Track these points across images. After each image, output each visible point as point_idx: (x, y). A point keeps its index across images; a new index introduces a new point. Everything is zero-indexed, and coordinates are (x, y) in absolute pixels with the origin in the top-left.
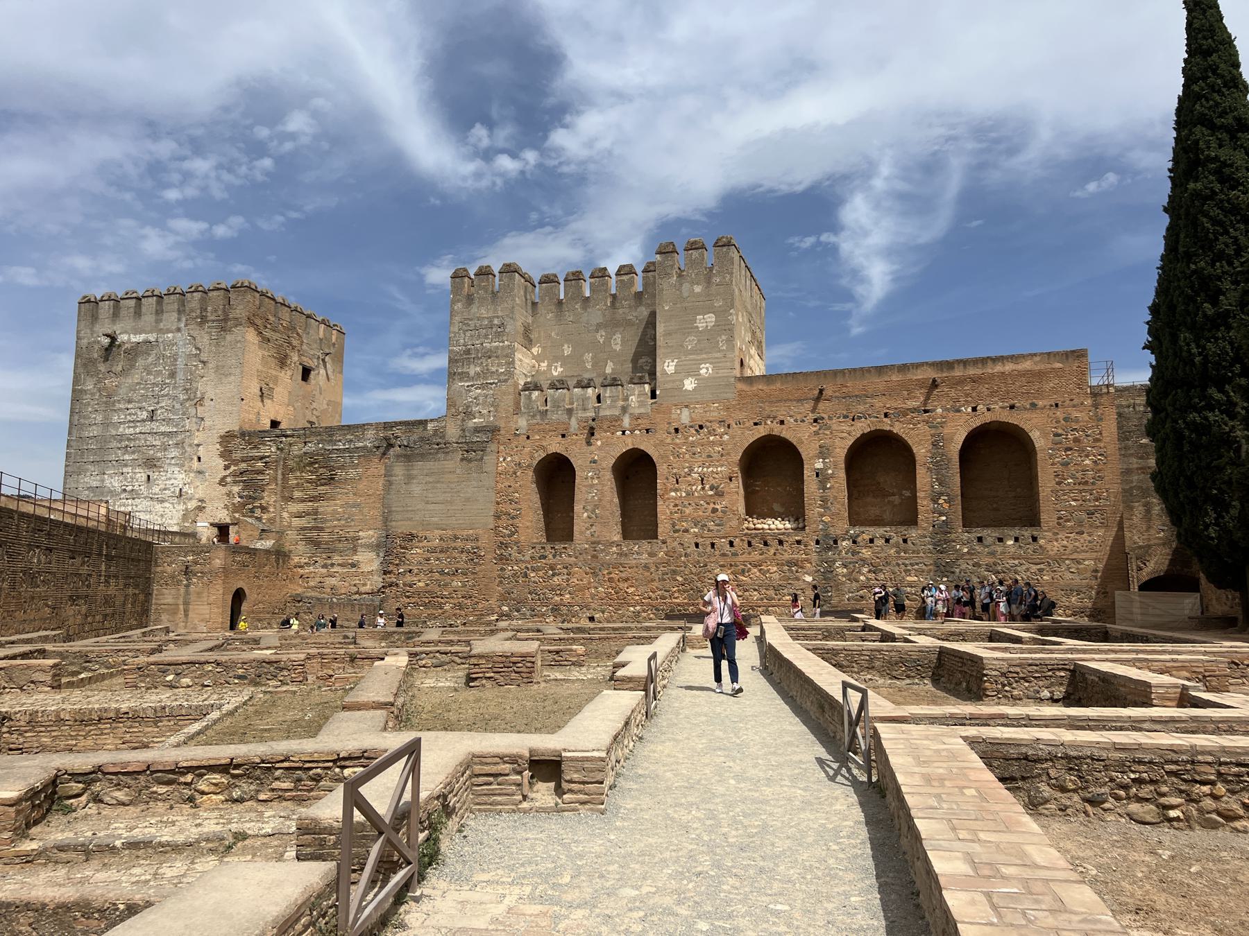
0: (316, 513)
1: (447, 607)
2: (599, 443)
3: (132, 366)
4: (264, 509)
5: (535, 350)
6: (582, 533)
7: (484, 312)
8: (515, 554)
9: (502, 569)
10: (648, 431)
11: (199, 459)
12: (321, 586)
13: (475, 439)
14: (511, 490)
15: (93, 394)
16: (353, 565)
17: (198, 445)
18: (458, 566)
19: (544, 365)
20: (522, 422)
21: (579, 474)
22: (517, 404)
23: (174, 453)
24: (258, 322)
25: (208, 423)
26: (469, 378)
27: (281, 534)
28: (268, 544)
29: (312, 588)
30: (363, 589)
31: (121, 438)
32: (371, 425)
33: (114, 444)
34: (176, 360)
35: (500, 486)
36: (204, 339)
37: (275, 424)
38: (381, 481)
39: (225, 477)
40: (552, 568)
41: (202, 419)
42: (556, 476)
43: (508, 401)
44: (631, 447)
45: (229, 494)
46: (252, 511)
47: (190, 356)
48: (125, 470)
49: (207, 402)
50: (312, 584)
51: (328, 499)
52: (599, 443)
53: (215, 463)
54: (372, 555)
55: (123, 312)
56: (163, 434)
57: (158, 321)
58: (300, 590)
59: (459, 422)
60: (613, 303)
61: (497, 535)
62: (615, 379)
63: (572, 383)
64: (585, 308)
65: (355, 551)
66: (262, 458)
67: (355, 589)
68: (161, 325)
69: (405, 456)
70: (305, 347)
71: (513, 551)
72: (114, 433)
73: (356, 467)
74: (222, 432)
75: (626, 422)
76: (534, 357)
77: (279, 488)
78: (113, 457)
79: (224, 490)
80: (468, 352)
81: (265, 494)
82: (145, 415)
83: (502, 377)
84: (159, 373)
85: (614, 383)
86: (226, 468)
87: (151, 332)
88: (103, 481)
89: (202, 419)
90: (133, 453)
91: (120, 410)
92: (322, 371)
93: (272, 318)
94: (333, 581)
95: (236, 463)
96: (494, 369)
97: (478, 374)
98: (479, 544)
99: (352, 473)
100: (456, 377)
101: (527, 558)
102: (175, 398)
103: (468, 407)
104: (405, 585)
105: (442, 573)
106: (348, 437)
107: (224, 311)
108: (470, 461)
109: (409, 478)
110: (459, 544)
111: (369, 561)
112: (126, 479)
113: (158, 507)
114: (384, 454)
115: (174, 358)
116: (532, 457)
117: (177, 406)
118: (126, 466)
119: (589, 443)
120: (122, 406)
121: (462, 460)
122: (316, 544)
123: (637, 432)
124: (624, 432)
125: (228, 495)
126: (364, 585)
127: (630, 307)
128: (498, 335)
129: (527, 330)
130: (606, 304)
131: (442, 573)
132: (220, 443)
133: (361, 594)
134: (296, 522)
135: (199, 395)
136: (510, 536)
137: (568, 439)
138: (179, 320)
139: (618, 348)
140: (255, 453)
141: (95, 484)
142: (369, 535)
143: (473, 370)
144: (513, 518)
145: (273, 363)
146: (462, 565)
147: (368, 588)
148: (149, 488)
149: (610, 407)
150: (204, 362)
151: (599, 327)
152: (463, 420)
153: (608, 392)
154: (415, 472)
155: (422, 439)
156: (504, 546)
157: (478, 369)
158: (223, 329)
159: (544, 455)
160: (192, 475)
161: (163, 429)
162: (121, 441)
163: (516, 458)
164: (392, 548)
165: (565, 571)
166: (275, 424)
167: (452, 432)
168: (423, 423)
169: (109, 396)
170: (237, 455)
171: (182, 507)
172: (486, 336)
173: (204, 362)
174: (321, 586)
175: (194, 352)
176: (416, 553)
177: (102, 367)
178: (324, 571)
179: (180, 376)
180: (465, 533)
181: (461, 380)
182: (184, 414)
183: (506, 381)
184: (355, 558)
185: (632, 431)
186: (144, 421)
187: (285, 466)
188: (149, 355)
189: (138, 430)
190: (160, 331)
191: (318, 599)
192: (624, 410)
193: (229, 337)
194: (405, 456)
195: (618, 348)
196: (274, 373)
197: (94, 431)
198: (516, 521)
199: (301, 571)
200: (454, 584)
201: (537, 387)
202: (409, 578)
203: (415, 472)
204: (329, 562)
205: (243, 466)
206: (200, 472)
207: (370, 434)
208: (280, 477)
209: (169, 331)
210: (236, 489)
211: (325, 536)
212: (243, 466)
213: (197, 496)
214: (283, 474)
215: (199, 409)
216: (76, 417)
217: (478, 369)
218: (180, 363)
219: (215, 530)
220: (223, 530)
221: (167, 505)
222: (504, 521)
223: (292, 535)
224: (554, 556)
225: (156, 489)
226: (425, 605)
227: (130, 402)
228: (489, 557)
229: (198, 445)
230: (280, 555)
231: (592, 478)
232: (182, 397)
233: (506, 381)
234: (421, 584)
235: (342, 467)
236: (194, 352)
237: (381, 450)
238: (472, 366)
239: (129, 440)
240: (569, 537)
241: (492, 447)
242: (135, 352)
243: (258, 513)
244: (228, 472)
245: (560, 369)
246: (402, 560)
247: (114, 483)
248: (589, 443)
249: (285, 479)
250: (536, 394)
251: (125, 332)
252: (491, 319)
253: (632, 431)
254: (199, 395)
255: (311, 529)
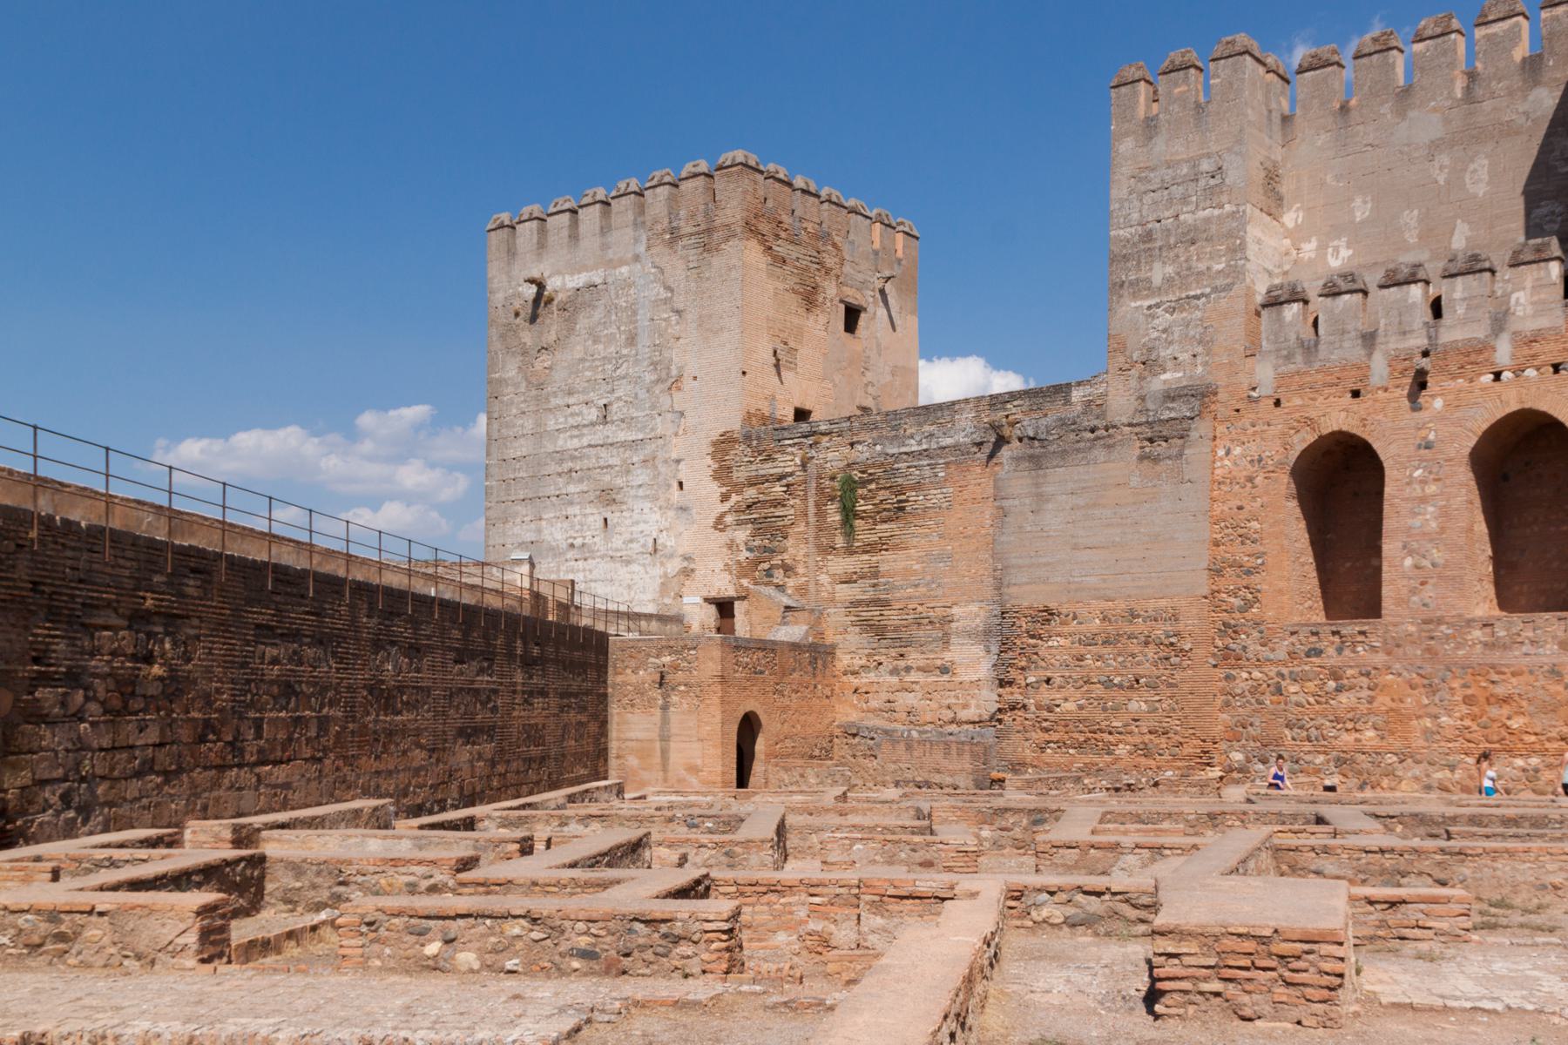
0: (876, 575)
1: (1122, 750)
2: (1438, 403)
3: (571, 330)
4: (788, 569)
5: (1290, 218)
6: (1400, 602)
7: (1179, 149)
8: (1254, 648)
9: (1228, 678)
10: (1556, 368)
11: (681, 484)
12: (889, 708)
13: (1166, 415)
14: (1244, 514)
15: (517, 385)
16: (944, 670)
17: (678, 461)
18: (1140, 670)
19: (1309, 248)
20: (1265, 374)
21: (1387, 472)
22: (1253, 336)
23: (641, 476)
24: (764, 227)
25: (690, 420)
26: (1152, 291)
27: (817, 616)
28: (793, 632)
29: (873, 711)
30: (964, 715)
31: (561, 457)
32: (966, 401)
33: (553, 468)
34: (635, 313)
35: (1218, 508)
36: (676, 266)
37: (801, 415)
38: (988, 512)
39: (722, 515)
40: (1335, 676)
41: (682, 414)
42: (1340, 486)
43: (1233, 332)
44: (1514, 407)
45: (731, 545)
46: (769, 573)
47: (657, 303)
48: (571, 511)
49: (688, 383)
50: (874, 704)
51: (896, 547)
52: (1438, 403)
53: (706, 492)
54: (978, 650)
55: (552, 239)
56: (623, 444)
57: (605, 247)
58: (854, 716)
59: (1133, 383)
60: (1468, 90)
61: (1216, 608)
62: (1475, 258)
63: (1372, 279)
64: (1401, 113)
65: (946, 641)
66: (781, 477)
67: (949, 715)
68: (610, 254)
69: (1031, 458)
70: (847, 269)
71: (1250, 642)
72: (550, 448)
73: (939, 485)
74: (715, 436)
75: (1503, 353)
76: (1288, 234)
77: (812, 532)
78: (552, 491)
79: (723, 538)
80: (1148, 237)
81: (789, 543)
82: (593, 414)
83: (1220, 282)
84: (611, 339)
85: (1474, 266)
86: (725, 498)
87: (595, 267)
88: (539, 531)
89: (682, 414)
90: (581, 480)
91: (558, 408)
92: (882, 312)
93: (786, 218)
94: (909, 700)
95: (738, 488)
96: (1202, 266)
97: (1169, 281)
98: (1181, 627)
99: (936, 497)
100: (1125, 292)
101: (1281, 654)
102: (637, 380)
103: (1150, 350)
104: (1039, 707)
105: (1108, 684)
106: (927, 428)
107: (706, 214)
108: (1156, 460)
109: (1041, 498)
110: (1140, 626)
111: (974, 663)
112: (572, 527)
113: (623, 572)
114: (991, 456)
116: (1286, 447)
117: (642, 395)
118: (571, 503)
119: (1415, 405)
120: (559, 401)
121: (1142, 458)
122: (878, 631)
123: (1531, 373)
124: (1497, 376)
125: (730, 547)
126: (965, 706)
127: (1511, 93)
129: (1272, 177)
130: (1450, 96)
131: (1108, 684)
132: (713, 455)
133: (960, 723)
134: (845, 592)
135: (674, 372)
136: (1243, 610)
137: (1366, 397)
138: (636, 240)
139: (1481, 190)
140: (769, 469)
141: (529, 537)
142: (971, 614)
143: (1159, 273)
144: (1249, 573)
145: (794, 302)
146: (1146, 669)
147: (971, 713)
148: (607, 540)
149: (1465, 321)
150: (678, 312)
152: (1141, 378)
153: (1457, 292)
154: (1048, 489)
155: (1062, 423)
156: (1230, 630)
157: (1170, 270)
158: (706, 248)
159: (1311, 438)
160: (671, 513)
161: (622, 436)
162: (562, 461)
163: (1253, 449)
164: (1015, 635)
165: (1364, 681)
166: (801, 415)
167: (1121, 403)
168: (1061, 391)
169: (540, 387)
170: (740, 475)
171: (657, 571)
172: (1184, 200)
173: (678, 312)
174: (889, 708)
175: (664, 294)
176: (1057, 646)
177: (527, 337)
178: (894, 680)
179: (644, 340)
180: (1151, 605)
181: (1135, 296)
182: (653, 407)
183: (1228, 288)
184: (948, 656)
185: (1518, 371)
186: (593, 424)
187: (820, 490)
188: (595, 307)
189: (585, 441)
190: (611, 264)
191: (886, 732)
192: (1499, 322)
193: (717, 261)
194: (1031, 458)
195: (1481, 190)
196: (796, 321)
197: (521, 448)
198: (1255, 579)
199: (855, 681)
200: (1133, 706)
201: (1297, 296)
202: (1046, 694)
203: (1048, 489)
204: (902, 664)
205: (751, 493)
206: (683, 509)
207: (966, 419)
208: (812, 510)
209: (622, 262)
210: (742, 535)
211: (892, 617)
212: (751, 493)
213: (681, 551)
214: (817, 505)
215: (677, 396)
216: (495, 426)
217: (1170, 270)
218: (643, 317)
219: (713, 609)
220: (724, 608)
221: (635, 567)
222: (1230, 580)
223: (836, 618)
224: (1340, 650)
225: (617, 542)
226: (1080, 746)
227: (570, 393)
228: (1200, 652)
229: (678, 461)
230: (817, 654)
231: (1423, 482)
232: (649, 377)
233: (1228, 288)
234: (1070, 706)
235: (918, 486)
236: (664, 294)
237: (987, 449)
238: (1157, 265)
239: (573, 458)
240: (1372, 608)
241: (1200, 428)
243: (779, 576)
244: (727, 506)
245: (1345, 253)
246: (1032, 656)
247: (556, 534)
248: (1415, 405)
249: (821, 514)
250: (1292, 311)
251: (559, 273)
252: (1194, 163)
253: (1518, 371)
254: (674, 372)
255: (869, 603)
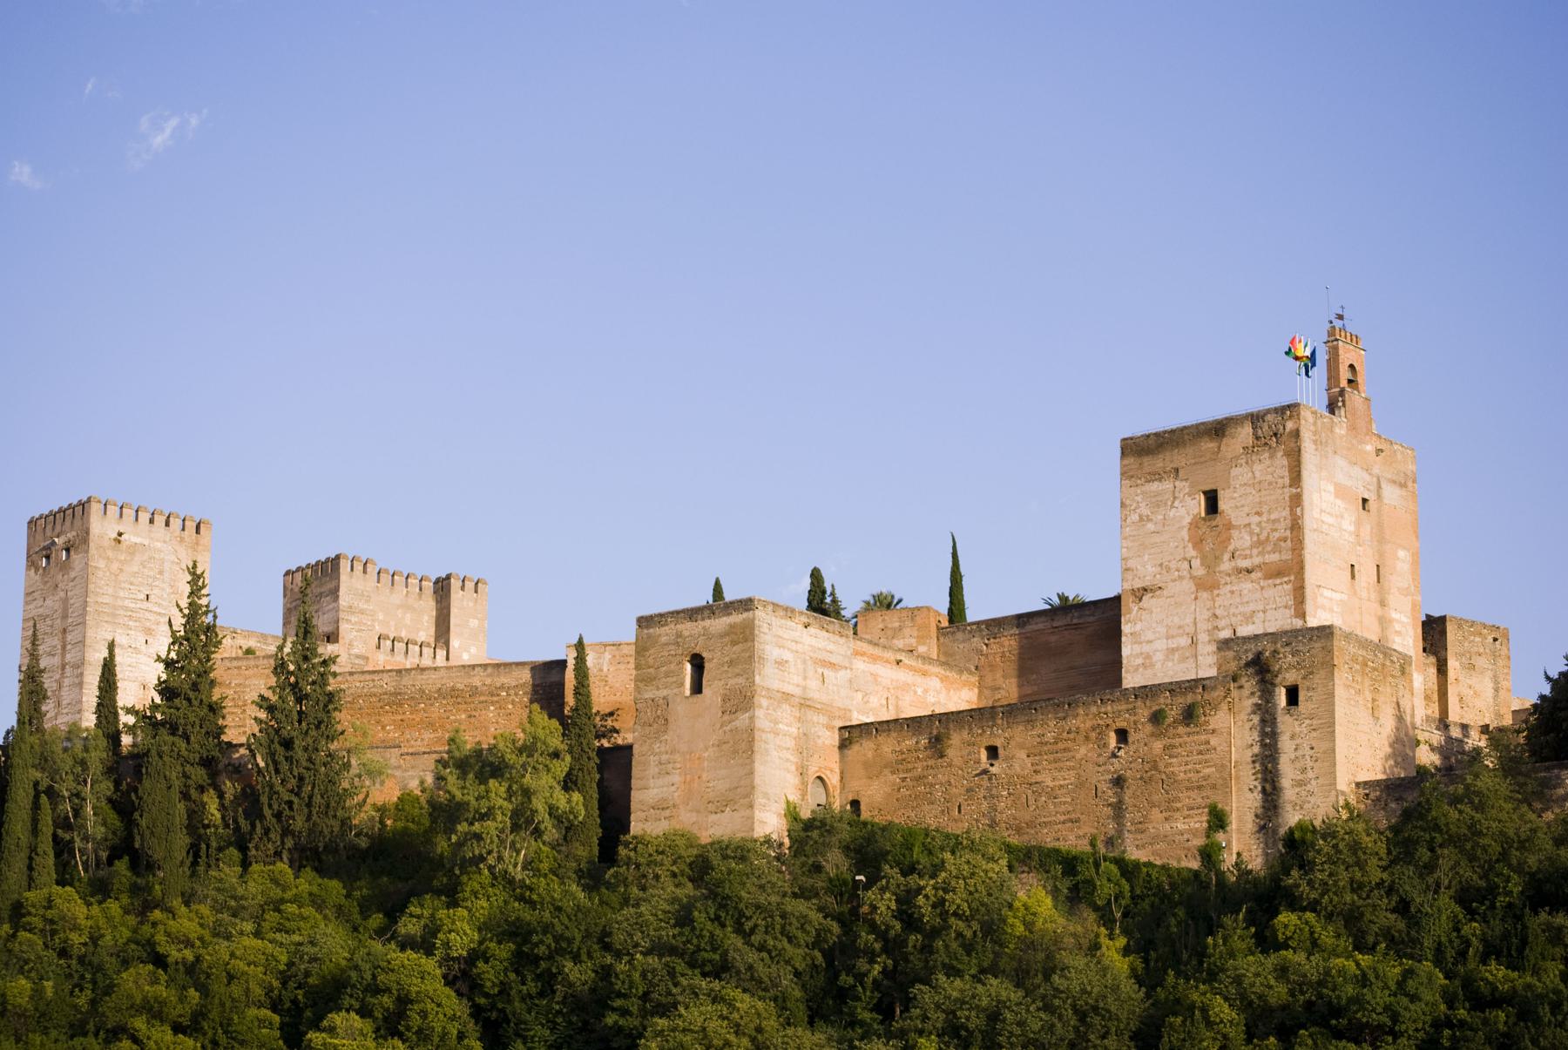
31: (126, 609)
82: (143, 596)
115: (162, 561)
128: (367, 601)
143: (354, 619)
151: (399, 607)
161: (156, 609)
177: (110, 553)
179: (166, 575)
197: (106, 600)
218: (167, 566)
242: (134, 549)
